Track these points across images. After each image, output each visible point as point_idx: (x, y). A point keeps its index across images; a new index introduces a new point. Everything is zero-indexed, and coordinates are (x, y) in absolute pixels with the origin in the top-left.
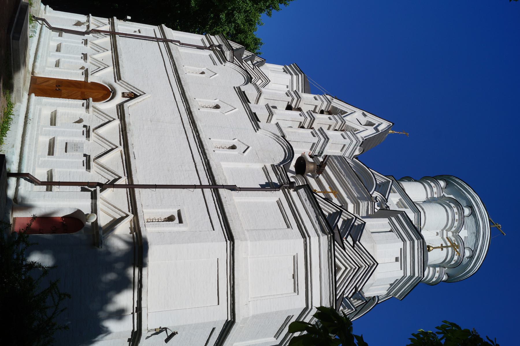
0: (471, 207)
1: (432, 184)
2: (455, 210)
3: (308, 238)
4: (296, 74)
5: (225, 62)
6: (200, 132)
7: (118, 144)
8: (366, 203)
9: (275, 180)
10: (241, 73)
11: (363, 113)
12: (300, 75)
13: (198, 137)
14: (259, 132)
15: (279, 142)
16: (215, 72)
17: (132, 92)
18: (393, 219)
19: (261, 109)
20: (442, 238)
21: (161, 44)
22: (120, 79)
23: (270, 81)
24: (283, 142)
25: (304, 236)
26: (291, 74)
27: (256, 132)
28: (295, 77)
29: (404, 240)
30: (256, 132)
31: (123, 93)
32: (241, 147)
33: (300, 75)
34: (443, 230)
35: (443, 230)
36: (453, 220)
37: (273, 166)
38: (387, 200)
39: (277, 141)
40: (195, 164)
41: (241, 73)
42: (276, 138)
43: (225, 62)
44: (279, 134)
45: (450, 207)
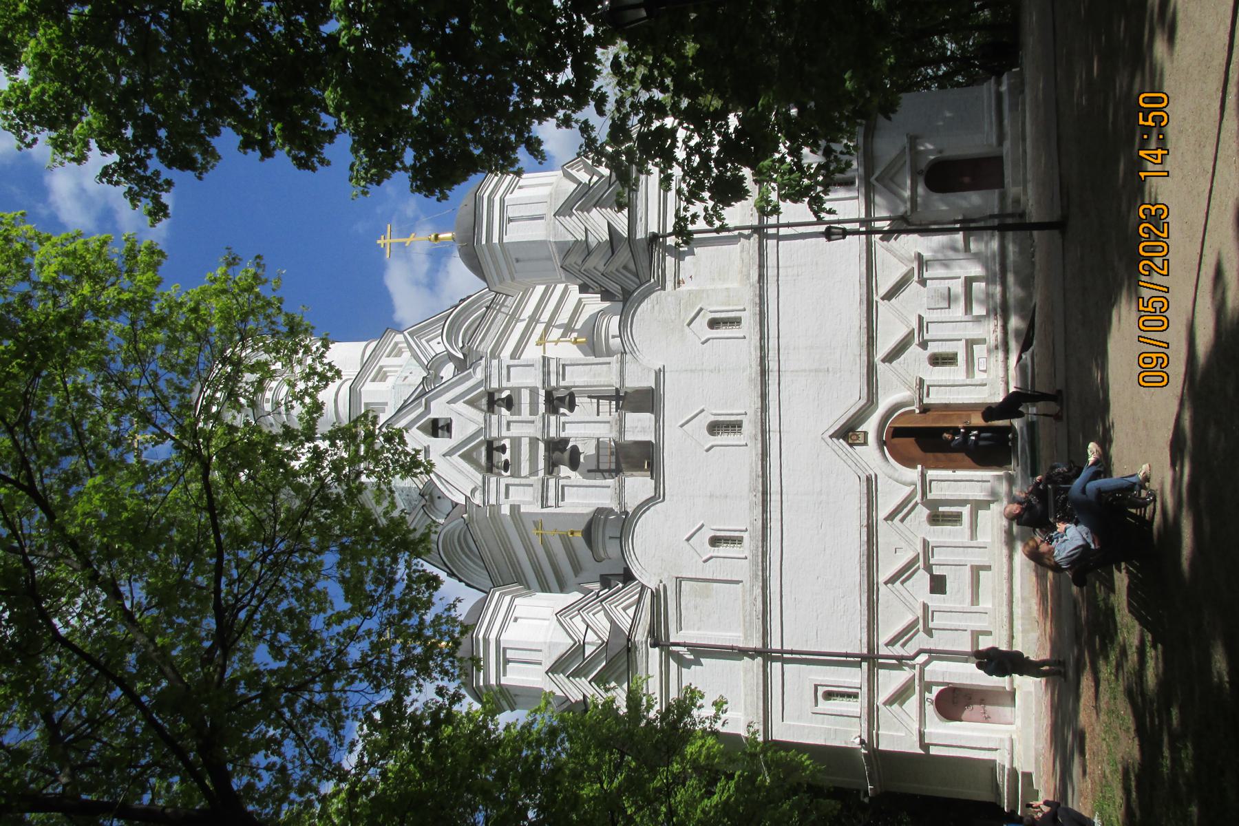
4: (486, 641)
5: (655, 596)
6: (758, 344)
7: (880, 301)
8: (481, 349)
9: (670, 261)
10: (633, 557)
12: (481, 636)
13: (762, 338)
16: (688, 547)
17: (851, 445)
18: (496, 240)
21: (776, 645)
22: (869, 479)
26: (498, 642)
28: (493, 637)
29: (502, 201)
31: (865, 443)
32: (703, 321)
33: (481, 636)
37: (664, 288)
38: (422, 383)
40: (778, 280)
41: (633, 557)
43: (658, 590)
44: (628, 357)
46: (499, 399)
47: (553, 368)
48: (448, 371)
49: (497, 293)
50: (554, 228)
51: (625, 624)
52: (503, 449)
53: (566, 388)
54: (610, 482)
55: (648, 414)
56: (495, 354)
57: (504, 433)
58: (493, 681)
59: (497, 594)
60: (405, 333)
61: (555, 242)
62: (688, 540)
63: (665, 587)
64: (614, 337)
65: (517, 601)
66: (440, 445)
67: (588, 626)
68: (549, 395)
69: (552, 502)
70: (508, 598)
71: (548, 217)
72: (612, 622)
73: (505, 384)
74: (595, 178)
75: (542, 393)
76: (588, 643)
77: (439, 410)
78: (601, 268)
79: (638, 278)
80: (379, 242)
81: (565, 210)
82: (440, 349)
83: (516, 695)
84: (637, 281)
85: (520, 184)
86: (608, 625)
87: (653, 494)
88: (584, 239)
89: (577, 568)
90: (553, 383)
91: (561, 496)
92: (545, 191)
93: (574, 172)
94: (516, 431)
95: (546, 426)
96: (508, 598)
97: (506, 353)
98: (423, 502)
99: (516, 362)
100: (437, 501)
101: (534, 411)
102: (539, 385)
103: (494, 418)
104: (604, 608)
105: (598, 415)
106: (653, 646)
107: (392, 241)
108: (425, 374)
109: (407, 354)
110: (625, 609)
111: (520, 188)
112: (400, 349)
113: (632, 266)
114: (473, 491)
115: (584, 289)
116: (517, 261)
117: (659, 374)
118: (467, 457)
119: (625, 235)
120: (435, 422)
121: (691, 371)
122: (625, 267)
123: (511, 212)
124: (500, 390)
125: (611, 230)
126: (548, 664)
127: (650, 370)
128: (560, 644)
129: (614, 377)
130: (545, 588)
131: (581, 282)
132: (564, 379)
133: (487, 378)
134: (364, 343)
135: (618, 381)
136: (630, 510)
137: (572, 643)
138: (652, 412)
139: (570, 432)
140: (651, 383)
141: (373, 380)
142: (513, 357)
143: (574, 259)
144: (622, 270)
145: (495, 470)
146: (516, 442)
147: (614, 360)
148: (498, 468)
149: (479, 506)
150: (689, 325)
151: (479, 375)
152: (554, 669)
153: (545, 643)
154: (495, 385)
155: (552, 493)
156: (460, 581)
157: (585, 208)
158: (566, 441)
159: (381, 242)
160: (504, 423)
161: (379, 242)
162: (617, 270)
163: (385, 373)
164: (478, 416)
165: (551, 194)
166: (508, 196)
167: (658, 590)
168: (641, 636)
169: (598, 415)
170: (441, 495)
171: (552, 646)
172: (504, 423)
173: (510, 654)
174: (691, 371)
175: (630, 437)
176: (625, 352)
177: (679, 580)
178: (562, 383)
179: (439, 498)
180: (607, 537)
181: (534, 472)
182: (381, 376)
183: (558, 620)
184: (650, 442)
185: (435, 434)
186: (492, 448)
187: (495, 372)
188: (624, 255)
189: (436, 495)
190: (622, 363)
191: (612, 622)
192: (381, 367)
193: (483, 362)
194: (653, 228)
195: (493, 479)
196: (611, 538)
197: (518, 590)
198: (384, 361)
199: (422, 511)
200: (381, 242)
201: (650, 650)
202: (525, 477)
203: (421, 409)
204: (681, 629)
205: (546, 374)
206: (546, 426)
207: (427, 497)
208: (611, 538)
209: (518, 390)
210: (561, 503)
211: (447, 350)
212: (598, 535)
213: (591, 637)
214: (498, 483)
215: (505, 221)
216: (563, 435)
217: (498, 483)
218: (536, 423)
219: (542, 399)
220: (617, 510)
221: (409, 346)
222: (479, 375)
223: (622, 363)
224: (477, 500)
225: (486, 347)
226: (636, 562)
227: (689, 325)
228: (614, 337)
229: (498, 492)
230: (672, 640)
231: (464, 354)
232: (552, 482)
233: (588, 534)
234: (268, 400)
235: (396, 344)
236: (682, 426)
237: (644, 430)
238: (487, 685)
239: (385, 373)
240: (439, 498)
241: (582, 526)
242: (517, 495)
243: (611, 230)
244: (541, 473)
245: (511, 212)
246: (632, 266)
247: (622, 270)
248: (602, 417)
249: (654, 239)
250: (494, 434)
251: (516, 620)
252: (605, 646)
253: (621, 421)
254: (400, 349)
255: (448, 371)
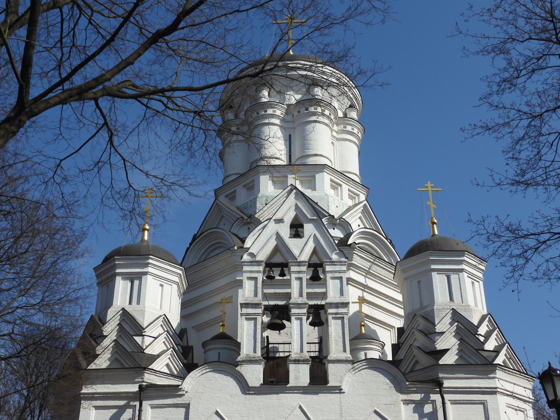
0: (315, 83)
1: (270, 111)
2: (319, 110)
3: (498, 390)
8: (355, 256)
10: (205, 371)
11: (275, 220)
12: (150, 261)
14: (344, 388)
15: (359, 369)
19: (299, 372)
20: (338, 139)
23: (165, 315)
24: (361, 365)
25: (494, 393)
26: (146, 273)
27: (344, 393)
30: (344, 393)
34: (333, 136)
35: (333, 136)
36: (328, 117)
38: (330, 215)
39: (357, 370)
42: (354, 370)
44: (350, 366)
45: (314, 114)
46: (318, 271)
47: (341, 310)
48: (337, 233)
49: (396, 266)
50: (444, 309)
51: (155, 366)
52: (282, 274)
53: (327, 320)
54: (259, 353)
55: (309, 381)
56: (351, 266)
57: (294, 276)
58: (118, 271)
59: (180, 272)
60: (366, 202)
61: (433, 310)
62: (217, 413)
63: (183, 395)
64: (366, 354)
65: (175, 287)
66: (285, 231)
67: (156, 338)
68: (322, 307)
69: (245, 311)
70: (177, 279)
71: (452, 304)
72: (158, 356)
73: (329, 275)
74: (482, 339)
75: (323, 303)
76: (143, 339)
77: (309, 229)
78: (416, 344)
79: (410, 372)
80: (429, 183)
81: (457, 317)
82: (355, 227)
83: (108, 286)
84: (407, 371)
85: (476, 283)
86: (156, 353)
87: (250, 385)
88: (437, 331)
89: (199, 328)
90: (330, 311)
91: (250, 318)
92: (471, 302)
93: (486, 322)
94: (295, 284)
95: (299, 306)
96: (177, 279)
97: (352, 274)
98: (245, 218)
99: (345, 282)
100: (246, 227)
101: (310, 296)
102: (329, 300)
103: (304, 268)
104: (168, 349)
105: (307, 343)
106: (140, 387)
107: (430, 192)
108: (336, 217)
109: (350, 203)
110: (167, 365)
111: (473, 283)
112: (354, 198)
113: (418, 367)
114: (252, 255)
115: (401, 331)
116: (419, 282)
117: (338, 390)
118: (276, 250)
119: (441, 362)
120: (302, 226)
121: (341, 414)
122: (417, 362)
123: (454, 277)
124: (324, 272)
125: (445, 351)
126: (129, 309)
127: (341, 382)
128: (143, 318)
129: (335, 356)
130: (184, 305)
131: (405, 329)
132: (333, 318)
133: (333, 263)
134: (358, 173)
135: (333, 358)
136: (238, 368)
137: (144, 327)
138: (310, 384)
139: (295, 323)
140: (332, 382)
141: (331, 180)
142: (349, 280)
143: (422, 324)
144: (415, 360)
145: (268, 269)
146: (288, 284)
147: (348, 355)
148: (269, 271)
149: (242, 258)
150: (376, 412)
151: (334, 257)
152: (125, 315)
153: (145, 307)
154: (328, 268)
155: (250, 311)
156: (191, 244)
157: (458, 334)
158: (289, 320)
159: (429, 184)
160: (301, 275)
161: (429, 183)
162: (414, 356)
163: (337, 188)
164: (305, 257)
165: (469, 306)
166: (465, 275)
167: (180, 390)
168: (149, 378)
169: (307, 343)
170: (251, 230)
171: (143, 312)
172: (301, 275)
173: (136, 283)
174: (341, 414)
175: (292, 367)
176: (353, 363)
177: (187, 407)
178: (330, 317)
179: (249, 229)
180: (220, 351)
181: (266, 296)
182: (335, 186)
183: (161, 316)
184: (288, 383)
185: (292, 226)
186: (283, 267)
187: (337, 268)
188: (425, 360)
189: (251, 226)
190: (346, 361)
191: (158, 356)
192: (340, 185)
193: (344, 259)
194: (447, 384)
195: (261, 268)
196: (219, 354)
197: (183, 286)
198: (345, 187)
199: (239, 217)
200: (429, 184)
201: (137, 385)
202: (262, 291)
203: (309, 217)
204: (152, 408)
205: (337, 305)
206: (299, 306)
207: (249, 220)
208: (219, 354)
209: (325, 285)
210: (244, 317)
211: (353, 232)
212: (219, 344)
213: (148, 340)
214: (258, 272)
215: (448, 273)
216: (293, 318)
217: (258, 272)
218: (301, 298)
219: (319, 302)
220: (239, 359)
221: (356, 205)
222: (334, 257)
223: (346, 361)
224: (246, 257)
225: (356, 260)
226: (201, 373)
227: (376, 412)
228: (366, 354)
229: (251, 272)
230: (144, 402)
231: (350, 245)
232: (260, 311)
233: (223, 337)
234: (316, 109)
235: (358, 195)
236: (300, 407)
237: (297, 378)
238: (115, 267)
239: (337, 188)
240: (249, 229)
241: (228, 333)
242: (248, 286)
243: (445, 351)
244: (266, 303)
245: (454, 278)
246: (418, 367)
247: (415, 360)
248: (306, 348)
249: (439, 384)
250: (293, 269)
251: (162, 285)
252: (141, 350)
253: (304, 361)
254: (354, 198)
255: (337, 233)
